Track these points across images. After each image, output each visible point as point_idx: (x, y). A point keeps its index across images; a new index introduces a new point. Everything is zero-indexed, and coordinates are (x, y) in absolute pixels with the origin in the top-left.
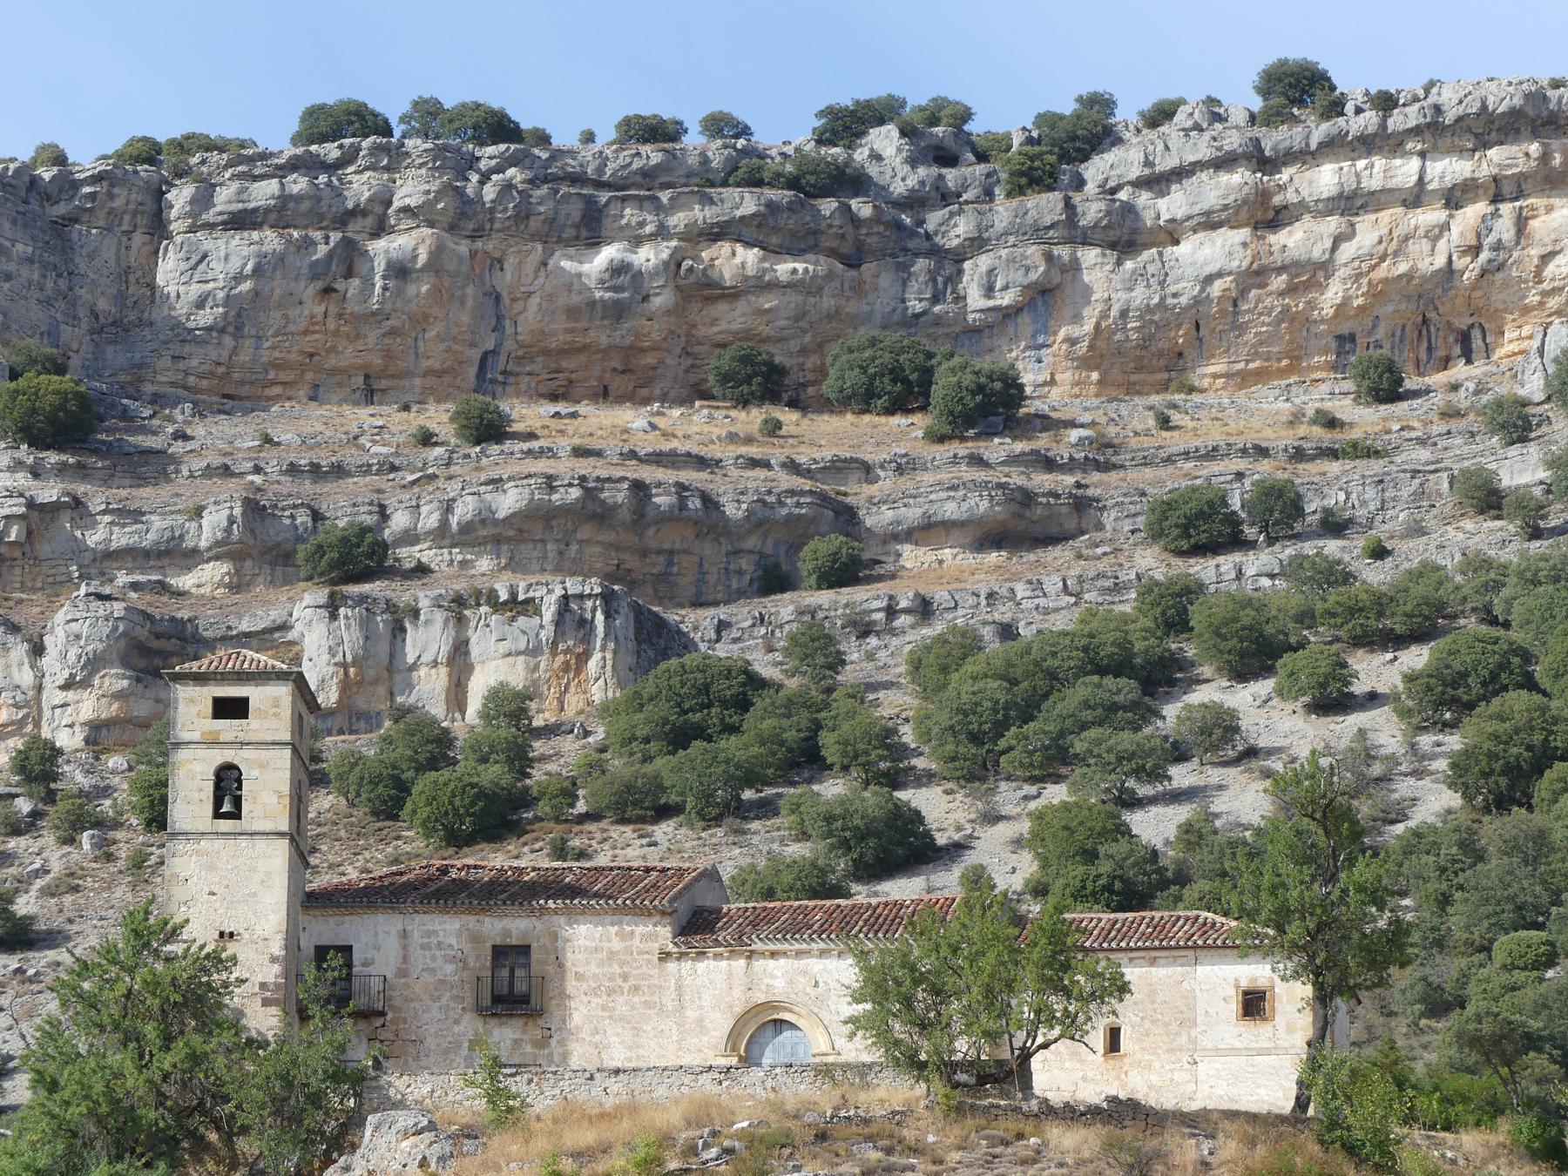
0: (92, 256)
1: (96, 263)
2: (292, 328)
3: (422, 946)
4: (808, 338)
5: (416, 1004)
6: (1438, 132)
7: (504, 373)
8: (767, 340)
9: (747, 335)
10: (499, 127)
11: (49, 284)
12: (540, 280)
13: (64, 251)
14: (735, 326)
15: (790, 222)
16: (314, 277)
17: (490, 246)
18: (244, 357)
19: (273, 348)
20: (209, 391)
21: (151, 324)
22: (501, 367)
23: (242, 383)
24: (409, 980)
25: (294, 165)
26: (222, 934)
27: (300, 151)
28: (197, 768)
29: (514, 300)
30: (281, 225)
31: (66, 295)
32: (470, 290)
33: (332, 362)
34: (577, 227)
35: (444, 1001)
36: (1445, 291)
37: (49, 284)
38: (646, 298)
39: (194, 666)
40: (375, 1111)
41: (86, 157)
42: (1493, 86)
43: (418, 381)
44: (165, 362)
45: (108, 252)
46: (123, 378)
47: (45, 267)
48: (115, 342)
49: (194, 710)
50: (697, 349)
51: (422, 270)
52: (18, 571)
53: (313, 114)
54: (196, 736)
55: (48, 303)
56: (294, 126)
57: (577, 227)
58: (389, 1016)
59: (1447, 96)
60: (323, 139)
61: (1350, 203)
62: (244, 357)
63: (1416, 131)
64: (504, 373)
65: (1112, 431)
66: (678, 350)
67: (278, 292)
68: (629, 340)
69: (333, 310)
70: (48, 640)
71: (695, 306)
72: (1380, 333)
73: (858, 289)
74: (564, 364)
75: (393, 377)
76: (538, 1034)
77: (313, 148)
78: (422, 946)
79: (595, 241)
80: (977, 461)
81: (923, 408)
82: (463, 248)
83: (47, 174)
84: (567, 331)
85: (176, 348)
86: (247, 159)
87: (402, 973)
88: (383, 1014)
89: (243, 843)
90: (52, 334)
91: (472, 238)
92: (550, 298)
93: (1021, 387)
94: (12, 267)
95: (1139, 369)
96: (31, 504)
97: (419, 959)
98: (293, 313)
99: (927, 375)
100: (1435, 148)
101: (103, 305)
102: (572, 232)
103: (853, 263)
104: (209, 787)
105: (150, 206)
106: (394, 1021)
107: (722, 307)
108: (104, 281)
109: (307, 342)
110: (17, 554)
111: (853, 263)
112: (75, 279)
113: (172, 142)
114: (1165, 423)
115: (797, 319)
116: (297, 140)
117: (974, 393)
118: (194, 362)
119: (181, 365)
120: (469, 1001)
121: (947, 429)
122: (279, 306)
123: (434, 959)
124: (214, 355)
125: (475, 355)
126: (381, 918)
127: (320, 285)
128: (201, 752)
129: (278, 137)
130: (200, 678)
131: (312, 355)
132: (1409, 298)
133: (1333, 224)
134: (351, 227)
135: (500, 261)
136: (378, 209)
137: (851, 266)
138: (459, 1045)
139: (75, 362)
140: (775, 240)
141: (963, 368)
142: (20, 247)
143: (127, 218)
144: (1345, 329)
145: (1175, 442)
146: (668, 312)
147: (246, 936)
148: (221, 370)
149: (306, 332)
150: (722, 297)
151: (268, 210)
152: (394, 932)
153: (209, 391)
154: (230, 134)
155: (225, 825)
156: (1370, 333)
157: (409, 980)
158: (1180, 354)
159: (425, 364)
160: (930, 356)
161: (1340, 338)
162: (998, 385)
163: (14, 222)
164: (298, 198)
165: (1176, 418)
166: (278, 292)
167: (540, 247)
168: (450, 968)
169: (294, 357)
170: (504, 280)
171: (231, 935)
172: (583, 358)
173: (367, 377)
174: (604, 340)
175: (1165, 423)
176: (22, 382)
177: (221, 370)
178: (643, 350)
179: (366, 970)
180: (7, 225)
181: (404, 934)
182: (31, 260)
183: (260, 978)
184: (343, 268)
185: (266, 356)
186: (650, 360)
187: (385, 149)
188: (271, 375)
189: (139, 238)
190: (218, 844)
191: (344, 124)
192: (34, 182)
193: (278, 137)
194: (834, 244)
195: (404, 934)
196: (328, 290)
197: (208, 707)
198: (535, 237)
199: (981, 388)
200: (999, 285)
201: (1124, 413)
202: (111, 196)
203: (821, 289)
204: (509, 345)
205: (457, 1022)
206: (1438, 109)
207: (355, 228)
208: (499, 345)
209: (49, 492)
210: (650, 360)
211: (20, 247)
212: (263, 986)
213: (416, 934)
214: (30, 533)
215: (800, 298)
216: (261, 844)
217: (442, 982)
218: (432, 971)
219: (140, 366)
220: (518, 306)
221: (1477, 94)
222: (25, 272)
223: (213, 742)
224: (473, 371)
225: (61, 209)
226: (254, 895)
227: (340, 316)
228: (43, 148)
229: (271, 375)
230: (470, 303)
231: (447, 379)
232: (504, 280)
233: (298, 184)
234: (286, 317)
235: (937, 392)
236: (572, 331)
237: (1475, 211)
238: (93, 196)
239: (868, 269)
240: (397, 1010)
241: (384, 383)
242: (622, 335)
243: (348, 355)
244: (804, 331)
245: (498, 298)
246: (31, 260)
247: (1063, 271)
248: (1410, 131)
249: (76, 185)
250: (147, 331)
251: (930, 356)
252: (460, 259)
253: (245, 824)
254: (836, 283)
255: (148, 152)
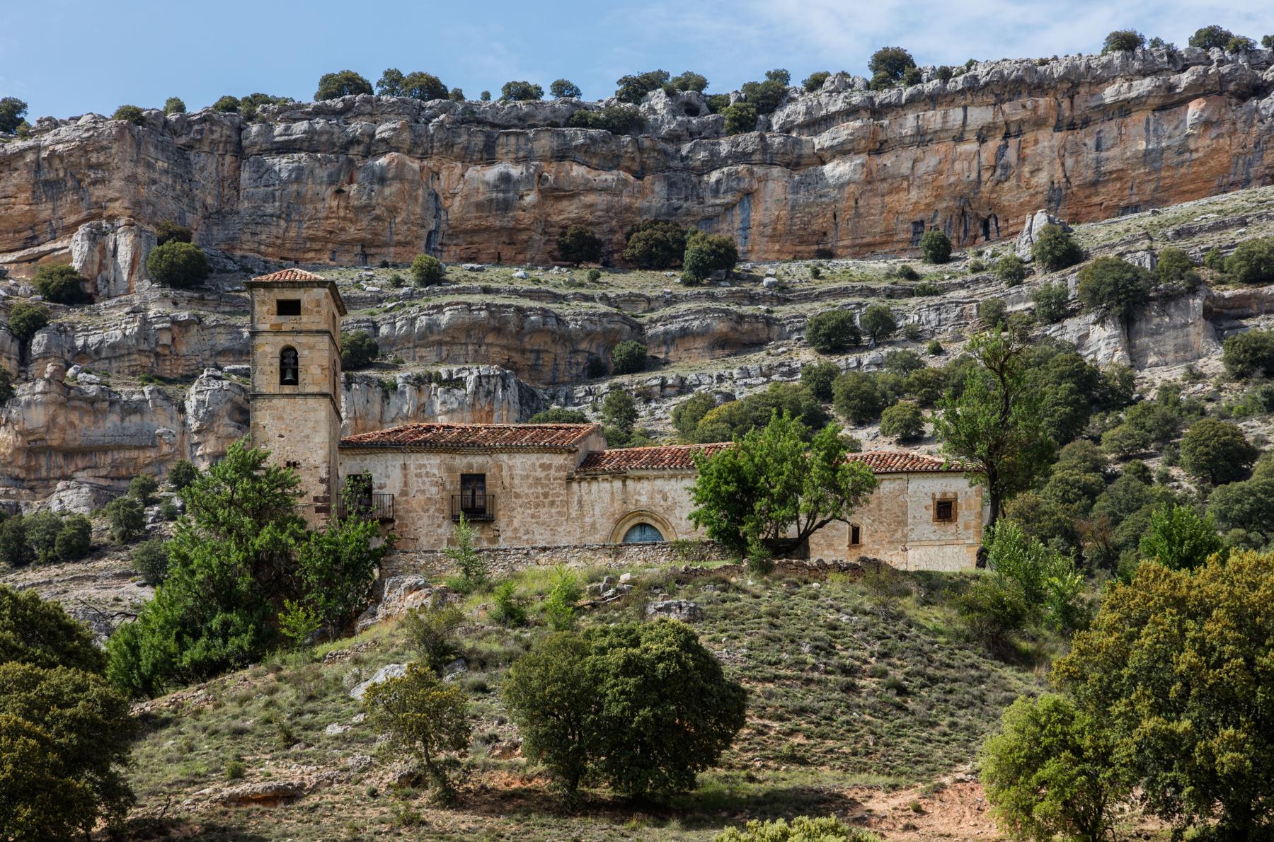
0: (202, 169)
1: (205, 174)
2: (320, 215)
3: (417, 475)
4: (614, 223)
5: (414, 514)
6: (974, 88)
7: (441, 244)
8: (591, 224)
9: (579, 220)
10: (433, 88)
11: (178, 188)
12: (461, 186)
13: (185, 166)
14: (573, 215)
15: (602, 149)
16: (331, 183)
17: (431, 164)
18: (292, 234)
19: (308, 228)
20: (273, 255)
21: (238, 213)
22: (440, 239)
23: (292, 250)
24: (409, 498)
25: (318, 112)
26: (288, 464)
27: (319, 103)
28: (268, 349)
29: (446, 198)
30: (312, 150)
31: (188, 194)
32: (420, 192)
33: (343, 237)
34: (481, 152)
35: (431, 512)
36: (976, 194)
37: (178, 188)
38: (521, 197)
39: (264, 278)
40: (390, 576)
41: (194, 108)
42: (1007, 64)
43: (392, 249)
44: (247, 237)
45: (211, 168)
46: (223, 246)
47: (175, 176)
48: (217, 224)
49: (265, 309)
50: (551, 230)
51: (392, 179)
52: (168, 363)
53: (326, 80)
54: (267, 327)
55: (177, 199)
56: (316, 89)
57: (481, 152)
58: (397, 522)
59: (980, 71)
60: (332, 96)
61: (922, 138)
62: (292, 234)
63: (962, 92)
64: (441, 244)
65: (786, 279)
66: (540, 230)
67: (310, 192)
68: (512, 224)
69: (342, 204)
70: (187, 404)
71: (549, 202)
72: (938, 220)
73: (642, 192)
74: (475, 239)
75: (379, 246)
76: (491, 534)
77: (328, 102)
78: (417, 475)
79: (491, 162)
80: (712, 297)
81: (680, 267)
82: (416, 165)
83: (172, 117)
84: (476, 218)
85: (253, 228)
86: (291, 111)
87: (404, 493)
88: (392, 521)
89: (300, 401)
90: (181, 218)
91: (421, 159)
92: (467, 197)
93: (735, 252)
94: (156, 176)
95: (801, 243)
96: (174, 322)
97: (415, 484)
98: (319, 206)
99: (682, 244)
100: (972, 103)
101: (209, 201)
102: (479, 156)
103: (639, 177)
104: (277, 362)
105: (235, 138)
106: (400, 526)
107: (565, 203)
108: (210, 186)
109: (327, 225)
110: (167, 352)
111: (639, 177)
112: (193, 184)
113: (245, 99)
114: (816, 274)
115: (607, 211)
116: (317, 97)
117: (708, 254)
118: (264, 237)
119: (256, 239)
120: (447, 513)
121: (693, 278)
122: (311, 201)
123: (424, 483)
124: (274, 232)
125: (424, 233)
126: (390, 456)
127: (334, 188)
128: (270, 338)
129: (307, 95)
130: (268, 286)
131: (331, 232)
132: (955, 198)
133: (914, 152)
134: (351, 152)
135: (437, 174)
136: (366, 140)
137: (638, 178)
138: (442, 542)
139: (195, 236)
140: (595, 161)
141: (703, 239)
142: (160, 163)
143: (221, 145)
144: (918, 218)
145: (824, 286)
146: (534, 206)
147: (303, 465)
148: (279, 241)
149: (327, 218)
150: (565, 196)
151: (302, 140)
152: (398, 466)
153: (273, 255)
154: (279, 96)
155: (288, 389)
156: (932, 221)
157: (409, 498)
158: (825, 234)
159: (396, 238)
160: (684, 233)
161: (915, 223)
162: (722, 251)
163: (156, 147)
164: (321, 133)
165: (823, 272)
166: (310, 192)
167: (460, 165)
168: (434, 490)
169: (320, 234)
170: (442, 185)
171: (295, 464)
172: (486, 236)
173: (363, 246)
174: (498, 223)
175: (816, 274)
176: (165, 246)
177: (279, 241)
178: (520, 230)
179: (381, 491)
180: (152, 149)
181: (405, 467)
182: (167, 172)
183: (314, 494)
184: (347, 178)
185: (305, 233)
186: (524, 236)
187: (368, 101)
188: (308, 245)
189: (228, 159)
190: (284, 402)
191: (344, 85)
192: (166, 122)
193: (307, 95)
194: (628, 164)
195: (405, 467)
196: (339, 192)
197: (274, 307)
198: (457, 158)
199: (713, 252)
200: (722, 190)
201: (794, 269)
202: (212, 132)
203: (621, 192)
204: (444, 226)
205: (439, 526)
206: (975, 78)
207: (354, 152)
208: (438, 226)
209: (184, 315)
210: (524, 236)
211: (160, 163)
212: (316, 499)
213: (412, 467)
214: (173, 339)
215: (609, 198)
216: (311, 402)
217: (429, 499)
218: (423, 492)
219: (233, 239)
220: (448, 203)
221: (997, 69)
222: (164, 179)
223: (277, 331)
224: (423, 243)
225: (183, 140)
226: (307, 437)
227: (346, 208)
228: (170, 101)
229: (308, 245)
230: (421, 200)
231: (409, 248)
232: (442, 185)
233: (320, 123)
234: (315, 208)
235: (688, 254)
236: (480, 218)
237: (993, 144)
238: (201, 132)
239: (648, 179)
240: (401, 518)
241: (373, 251)
242: (507, 222)
243: (352, 231)
244: (612, 219)
245: (437, 197)
246: (167, 172)
247: (759, 181)
248: (959, 92)
249: (190, 124)
250: (236, 218)
251: (684, 233)
252: (414, 171)
253: (300, 389)
254: (630, 189)
255: (229, 105)
